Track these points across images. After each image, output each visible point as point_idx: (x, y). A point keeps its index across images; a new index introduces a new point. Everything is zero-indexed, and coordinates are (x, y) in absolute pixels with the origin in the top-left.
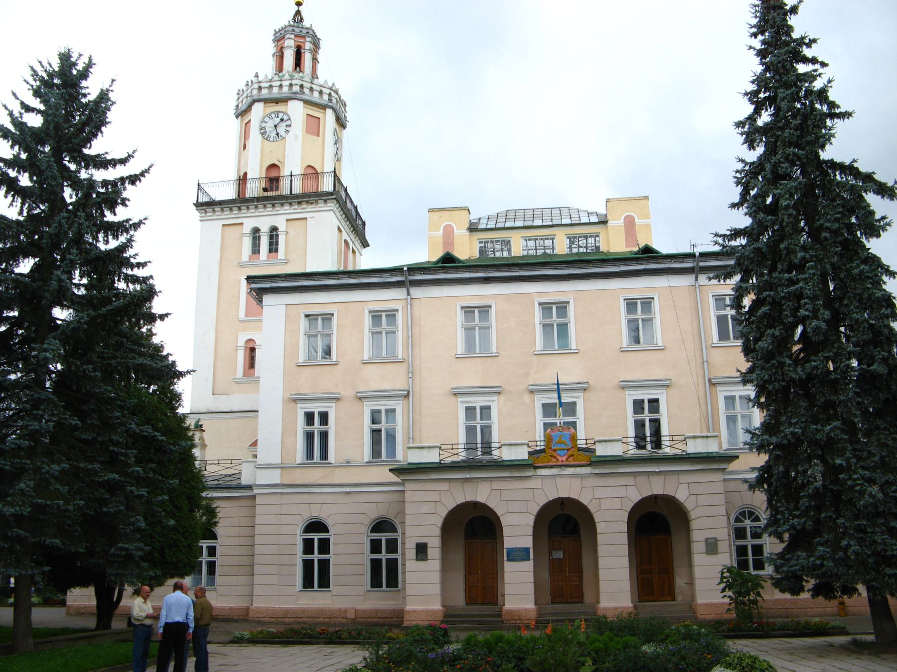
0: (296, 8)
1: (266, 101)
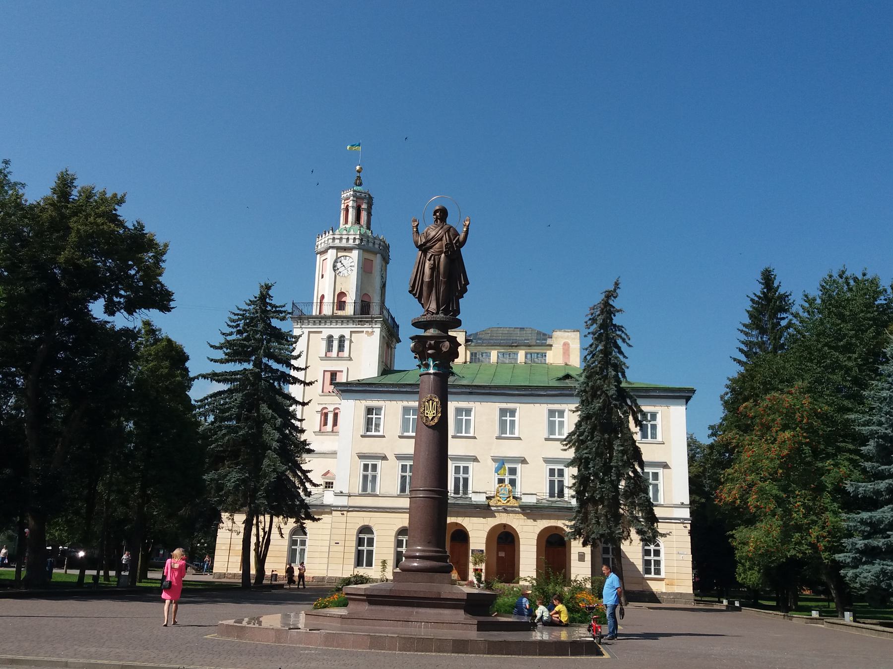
1: (339, 249)
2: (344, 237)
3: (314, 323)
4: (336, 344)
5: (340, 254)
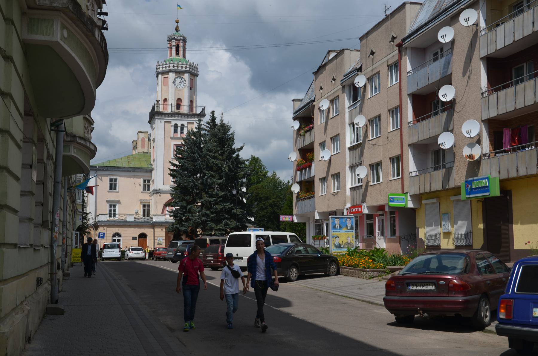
0: (176, 24)
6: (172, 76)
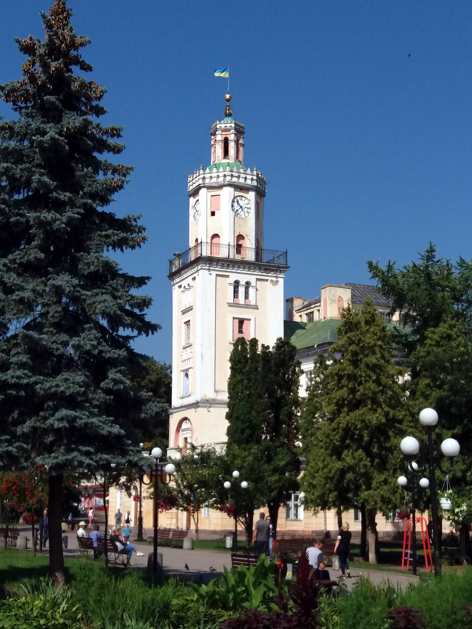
2: (242, 175)
3: (222, 266)
4: (241, 290)
5: (237, 193)
6: (228, 193)
